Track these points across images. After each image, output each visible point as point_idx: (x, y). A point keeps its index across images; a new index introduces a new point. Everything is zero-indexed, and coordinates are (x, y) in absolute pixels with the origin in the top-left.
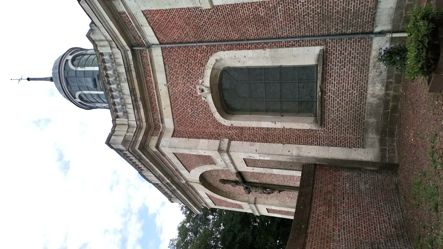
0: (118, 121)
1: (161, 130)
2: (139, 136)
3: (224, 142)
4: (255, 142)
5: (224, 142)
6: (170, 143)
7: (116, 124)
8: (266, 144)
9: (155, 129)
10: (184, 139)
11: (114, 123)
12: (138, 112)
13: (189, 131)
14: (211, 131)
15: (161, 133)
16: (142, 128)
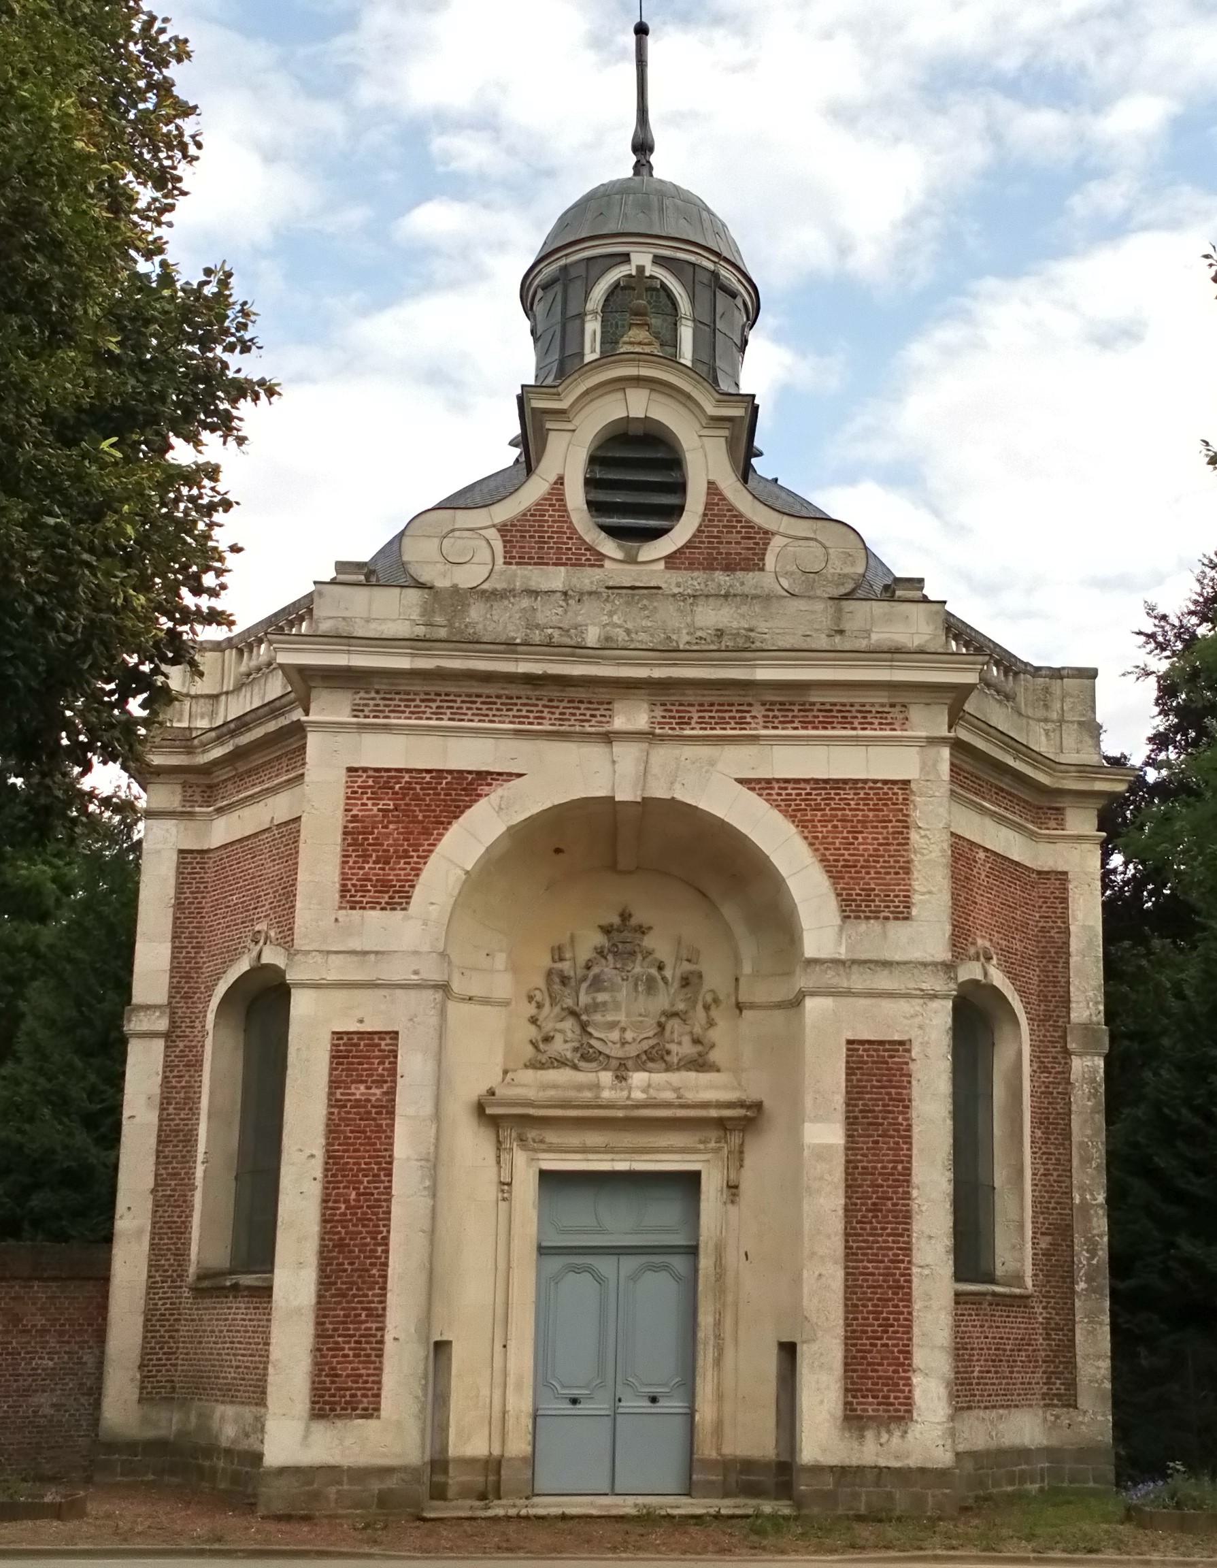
0: (231, 655)
1: (197, 809)
2: (163, 753)
3: (159, 1017)
4: (162, 1109)
5: (159, 1017)
6: (158, 852)
7: (223, 651)
8: (153, 1141)
9: (210, 787)
10: (172, 892)
11: (224, 645)
12: (219, 741)
13: (204, 898)
14: (200, 968)
15: (191, 814)
16: (189, 753)
